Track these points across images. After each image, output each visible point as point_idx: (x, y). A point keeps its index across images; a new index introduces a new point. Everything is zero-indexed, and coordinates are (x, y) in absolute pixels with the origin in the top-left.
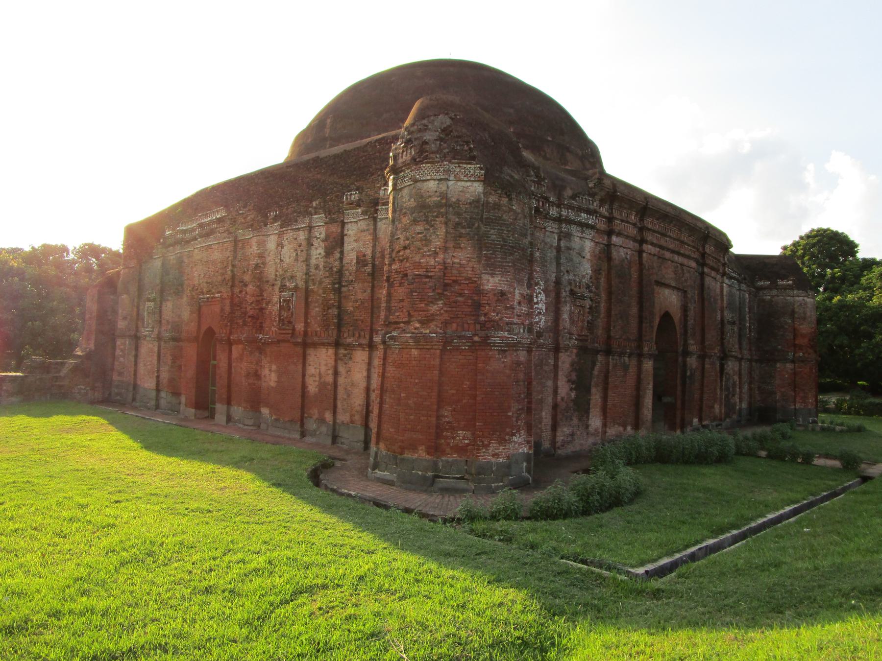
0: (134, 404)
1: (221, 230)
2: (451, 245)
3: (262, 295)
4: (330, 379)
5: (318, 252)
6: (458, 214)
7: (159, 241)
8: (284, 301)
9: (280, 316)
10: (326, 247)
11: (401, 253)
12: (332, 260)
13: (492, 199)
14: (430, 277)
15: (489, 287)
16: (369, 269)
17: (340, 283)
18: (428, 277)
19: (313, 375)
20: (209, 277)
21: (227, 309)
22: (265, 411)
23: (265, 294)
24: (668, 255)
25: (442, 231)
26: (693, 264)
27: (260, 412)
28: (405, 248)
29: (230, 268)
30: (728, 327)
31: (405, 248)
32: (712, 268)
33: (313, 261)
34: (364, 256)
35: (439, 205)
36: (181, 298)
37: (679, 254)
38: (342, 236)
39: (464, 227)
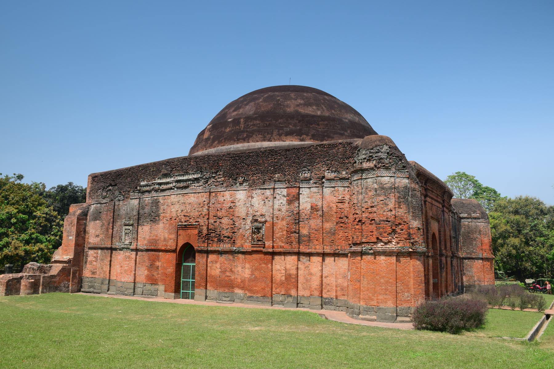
0: (109, 292)
1: (196, 185)
2: (397, 206)
3: (234, 224)
4: (294, 272)
5: (280, 201)
6: (399, 192)
7: (136, 188)
8: (255, 228)
9: (252, 237)
10: (287, 200)
11: (369, 209)
12: (293, 207)
13: (413, 186)
14: (389, 221)
15: (414, 226)
16: (320, 213)
17: (298, 220)
18: (387, 221)
19: (279, 270)
20: (187, 212)
21: (205, 232)
22: (239, 292)
23: (237, 224)
24: (434, 202)
25: (393, 200)
26: (441, 206)
27: (233, 292)
28: (372, 207)
29: (206, 207)
30: (453, 240)
31: (372, 207)
32: (447, 208)
33: (276, 207)
34: (317, 206)
35: (391, 188)
36: (158, 224)
37: (436, 200)
38: (299, 194)
39: (402, 198)
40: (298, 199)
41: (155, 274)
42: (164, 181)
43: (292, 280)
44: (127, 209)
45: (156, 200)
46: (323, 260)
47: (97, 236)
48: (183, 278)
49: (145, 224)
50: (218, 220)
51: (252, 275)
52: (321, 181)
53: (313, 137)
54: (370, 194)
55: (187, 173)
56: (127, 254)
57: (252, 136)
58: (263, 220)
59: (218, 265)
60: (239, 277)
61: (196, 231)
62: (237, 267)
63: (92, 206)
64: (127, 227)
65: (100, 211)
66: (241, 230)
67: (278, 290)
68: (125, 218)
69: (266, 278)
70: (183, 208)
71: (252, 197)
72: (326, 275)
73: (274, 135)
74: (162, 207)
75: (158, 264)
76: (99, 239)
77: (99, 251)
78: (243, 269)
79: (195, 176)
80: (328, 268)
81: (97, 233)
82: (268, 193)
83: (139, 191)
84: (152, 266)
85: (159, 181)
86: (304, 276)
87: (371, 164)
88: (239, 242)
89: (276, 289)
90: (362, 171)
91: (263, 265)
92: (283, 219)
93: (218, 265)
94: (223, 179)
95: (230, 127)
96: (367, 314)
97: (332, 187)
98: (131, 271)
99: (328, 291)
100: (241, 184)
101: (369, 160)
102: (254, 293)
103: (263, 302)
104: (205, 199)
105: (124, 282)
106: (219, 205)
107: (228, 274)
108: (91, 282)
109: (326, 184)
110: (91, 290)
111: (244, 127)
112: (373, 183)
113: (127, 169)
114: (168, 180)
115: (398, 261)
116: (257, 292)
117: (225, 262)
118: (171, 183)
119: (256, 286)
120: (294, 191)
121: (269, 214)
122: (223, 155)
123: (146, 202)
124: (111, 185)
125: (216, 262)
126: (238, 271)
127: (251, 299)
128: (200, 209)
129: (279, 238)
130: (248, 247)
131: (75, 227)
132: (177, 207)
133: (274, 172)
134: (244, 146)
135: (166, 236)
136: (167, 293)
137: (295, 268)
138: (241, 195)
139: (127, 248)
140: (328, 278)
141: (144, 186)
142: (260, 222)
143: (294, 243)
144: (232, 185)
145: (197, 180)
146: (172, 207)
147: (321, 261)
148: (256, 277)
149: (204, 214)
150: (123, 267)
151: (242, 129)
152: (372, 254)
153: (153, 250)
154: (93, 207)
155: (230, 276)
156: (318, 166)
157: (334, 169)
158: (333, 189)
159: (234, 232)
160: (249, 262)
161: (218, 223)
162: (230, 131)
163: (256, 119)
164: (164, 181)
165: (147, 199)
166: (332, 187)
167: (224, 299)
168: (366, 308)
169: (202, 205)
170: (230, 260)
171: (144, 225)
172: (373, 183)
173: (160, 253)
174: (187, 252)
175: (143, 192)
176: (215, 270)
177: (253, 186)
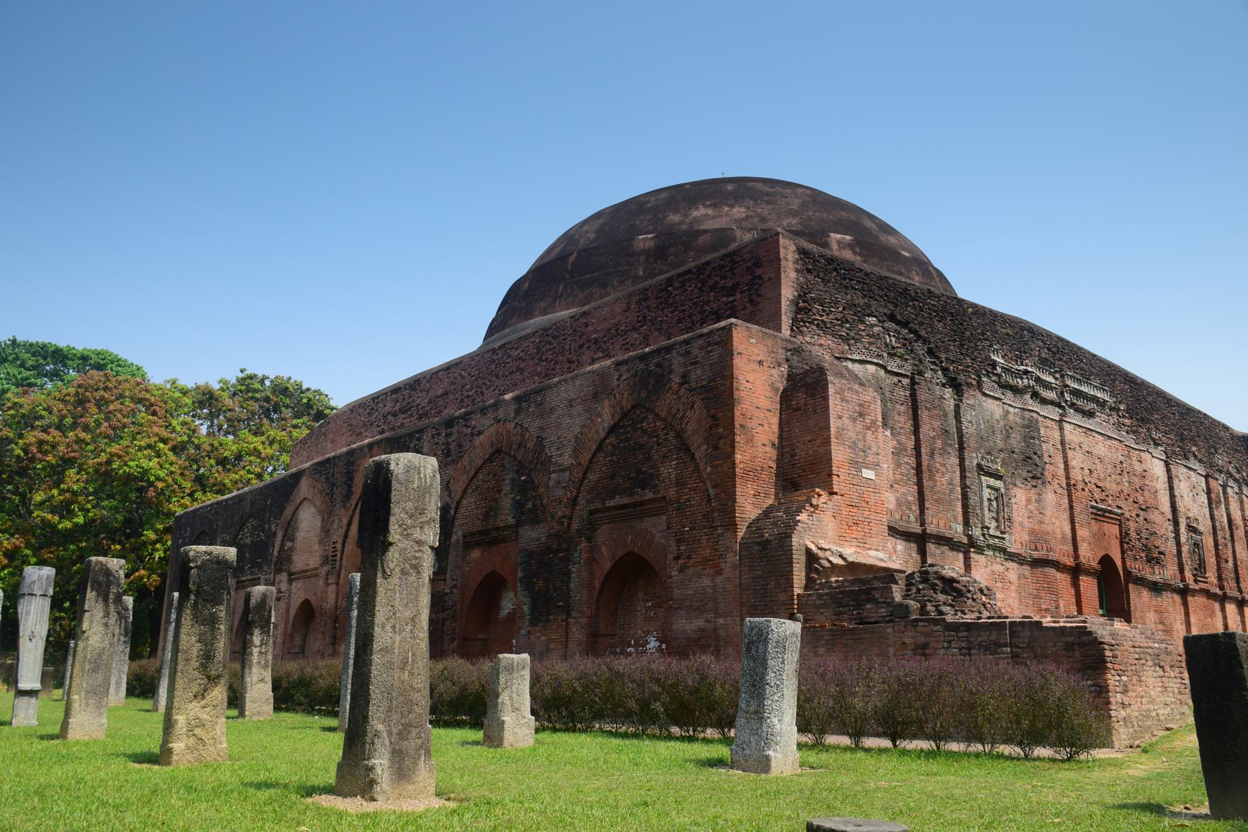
49: (1018, 482)
50: (1141, 513)
64: (992, 481)
68: (977, 450)
77: (900, 545)
100: (1156, 445)
104: (1121, 458)
123: (1011, 417)
139: (995, 548)
145: (1102, 404)
165: (1011, 409)
173: (1059, 575)
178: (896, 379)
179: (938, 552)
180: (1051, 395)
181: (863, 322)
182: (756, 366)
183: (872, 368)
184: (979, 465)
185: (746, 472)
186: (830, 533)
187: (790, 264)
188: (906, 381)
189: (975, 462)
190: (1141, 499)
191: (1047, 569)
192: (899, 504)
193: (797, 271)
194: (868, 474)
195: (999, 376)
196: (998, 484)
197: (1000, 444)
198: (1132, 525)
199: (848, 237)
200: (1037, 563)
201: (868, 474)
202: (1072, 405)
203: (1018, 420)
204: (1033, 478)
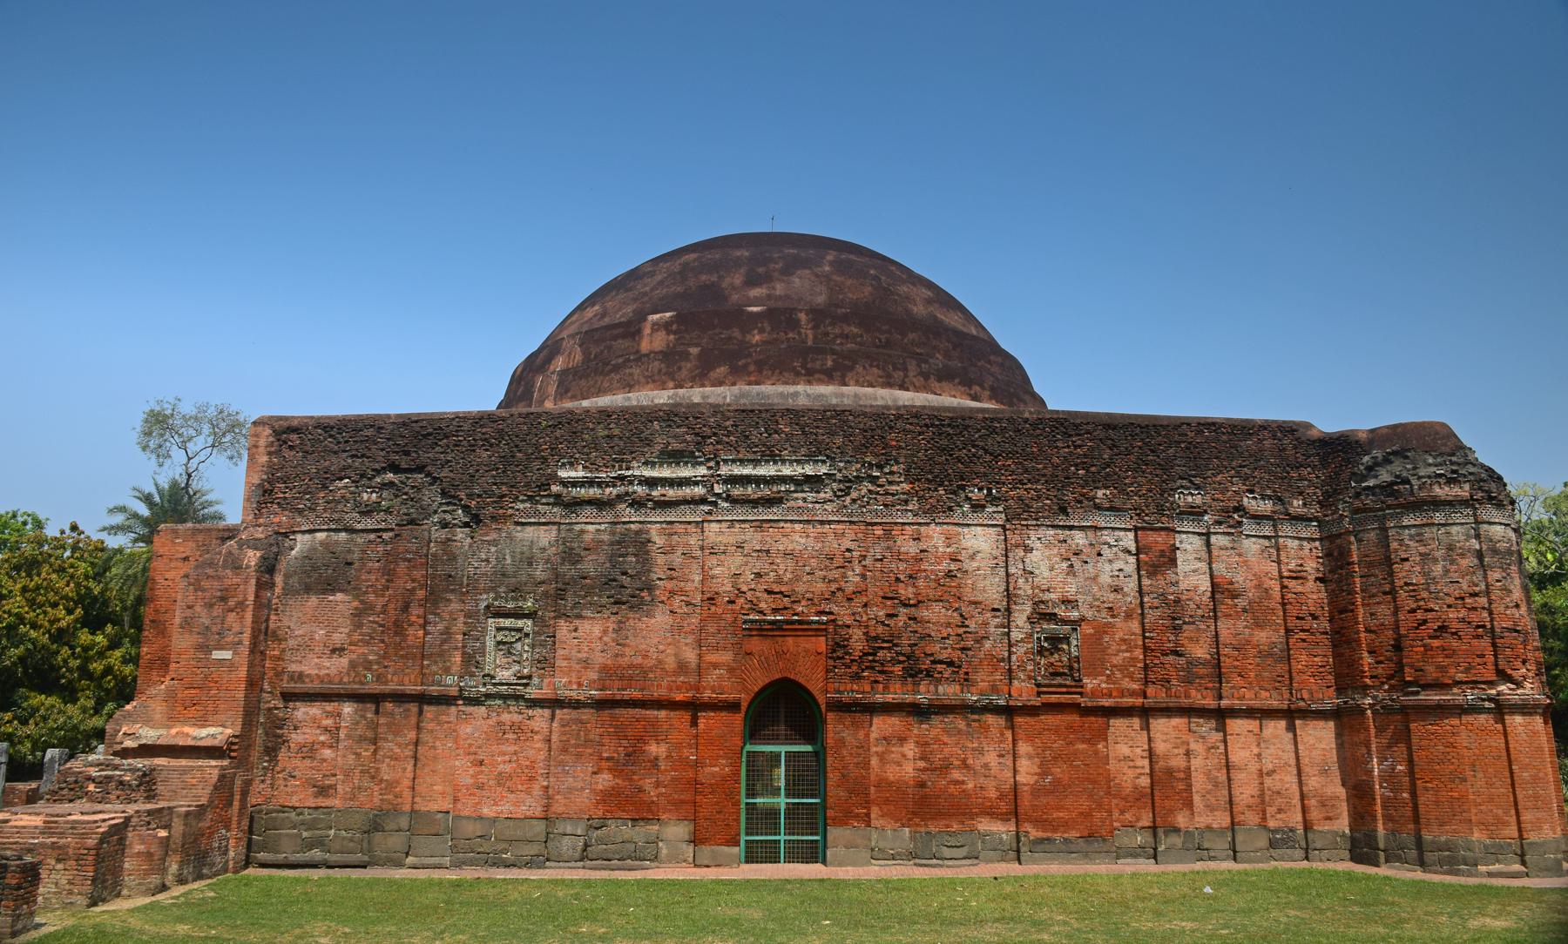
0: (410, 860)
1: (811, 496)
5: (1117, 565)
23: (972, 626)
34: (1232, 583)
40: (1173, 562)
41: (647, 783)
42: (666, 472)
43: (1165, 788)
44: (500, 559)
45: (637, 533)
46: (1222, 728)
47: (338, 651)
48: (748, 796)
51: (1043, 774)
52: (1232, 517)
53: (995, 395)
54: (1465, 562)
55: (772, 457)
56: (506, 717)
57: (851, 369)
58: (1075, 614)
59: (910, 749)
60: (991, 785)
61: (821, 644)
62: (981, 752)
63: (299, 537)
64: (507, 622)
65: (349, 558)
66: (988, 644)
67: (1128, 816)
68: (493, 589)
69: (1094, 782)
70: (759, 566)
71: (1028, 549)
72: (1270, 767)
73: (911, 374)
74: (661, 559)
75: (655, 749)
76: (344, 662)
77: (348, 709)
78: (998, 761)
79: (809, 470)
80: (1272, 750)
81: (339, 638)
82: (1079, 539)
83: (558, 500)
84: (631, 760)
85: (648, 473)
86: (1208, 774)
87: (1463, 491)
88: (983, 679)
89: (1122, 812)
90: (1437, 504)
91: (1081, 746)
92: (1128, 616)
93: (910, 749)
94: (906, 487)
95: (761, 331)
96: (1498, 861)
97: (1264, 537)
98: (532, 779)
99: (1280, 811)
100: (977, 507)
101: (1450, 481)
102: (1055, 830)
103: (1087, 856)
104: (847, 544)
105: (494, 820)
106: (902, 566)
107: (956, 775)
108: (311, 826)
109: (1249, 527)
110: (316, 854)
111: (815, 337)
112: (1468, 537)
113: (460, 418)
114: (686, 472)
115: (1291, 728)
116: (1066, 825)
117: (945, 739)
118: (696, 483)
119: (1059, 808)
120: (1159, 538)
121: (1089, 599)
122: (898, 417)
124: (395, 468)
125: (902, 740)
126: (986, 766)
127: (1047, 847)
128: (836, 574)
129: (1122, 668)
130: (1023, 691)
131: (249, 616)
132: (735, 562)
133: (1095, 482)
134: (843, 395)
135: (690, 656)
136: (706, 851)
137: (1181, 751)
138: (980, 540)
140: (1277, 777)
141: (574, 484)
142: (1065, 622)
143: (1174, 682)
144: (950, 509)
145: (814, 482)
146: (713, 561)
147: (1256, 730)
148: (1057, 782)
149: (850, 588)
150: (475, 765)
151: (810, 343)
152: (1489, 711)
153: (620, 704)
154: (302, 543)
155: (963, 782)
156: (1219, 478)
157: (1269, 492)
158: (1267, 543)
159: (963, 649)
160: (1030, 739)
161: (901, 620)
162: (765, 343)
163: (845, 319)
164: (666, 472)
165: (590, 528)
166: (1264, 537)
167: (947, 852)
168: (1493, 846)
169: (839, 561)
170: (960, 731)
171: (579, 617)
172: (1468, 537)
173: (662, 714)
174: (783, 707)
175: (576, 504)
176: (899, 764)
177: (1018, 516)
178: (372, 536)
179: (397, 710)
180: (699, 491)
181: (325, 487)
182: (180, 564)
183: (321, 536)
184: (487, 607)
185: (151, 662)
186: (157, 717)
187: (262, 450)
188: (386, 536)
189: (483, 605)
190: (906, 592)
191: (617, 711)
192: (353, 665)
193: (270, 454)
194: (217, 655)
195: (558, 496)
196: (520, 623)
197: (539, 573)
198: (857, 633)
199: (668, 314)
200: (601, 704)
201: (217, 655)
202: (729, 498)
203: (606, 537)
204: (616, 603)
